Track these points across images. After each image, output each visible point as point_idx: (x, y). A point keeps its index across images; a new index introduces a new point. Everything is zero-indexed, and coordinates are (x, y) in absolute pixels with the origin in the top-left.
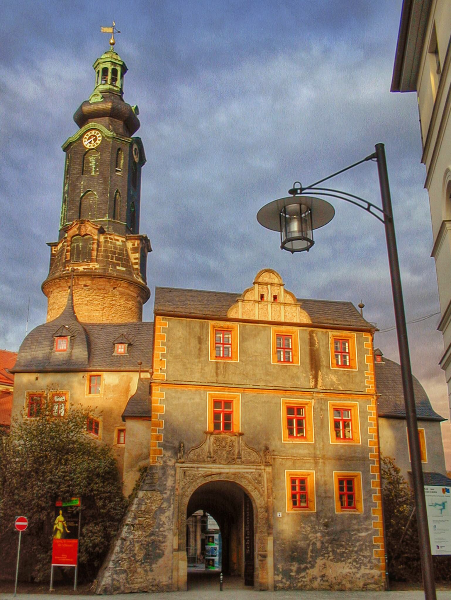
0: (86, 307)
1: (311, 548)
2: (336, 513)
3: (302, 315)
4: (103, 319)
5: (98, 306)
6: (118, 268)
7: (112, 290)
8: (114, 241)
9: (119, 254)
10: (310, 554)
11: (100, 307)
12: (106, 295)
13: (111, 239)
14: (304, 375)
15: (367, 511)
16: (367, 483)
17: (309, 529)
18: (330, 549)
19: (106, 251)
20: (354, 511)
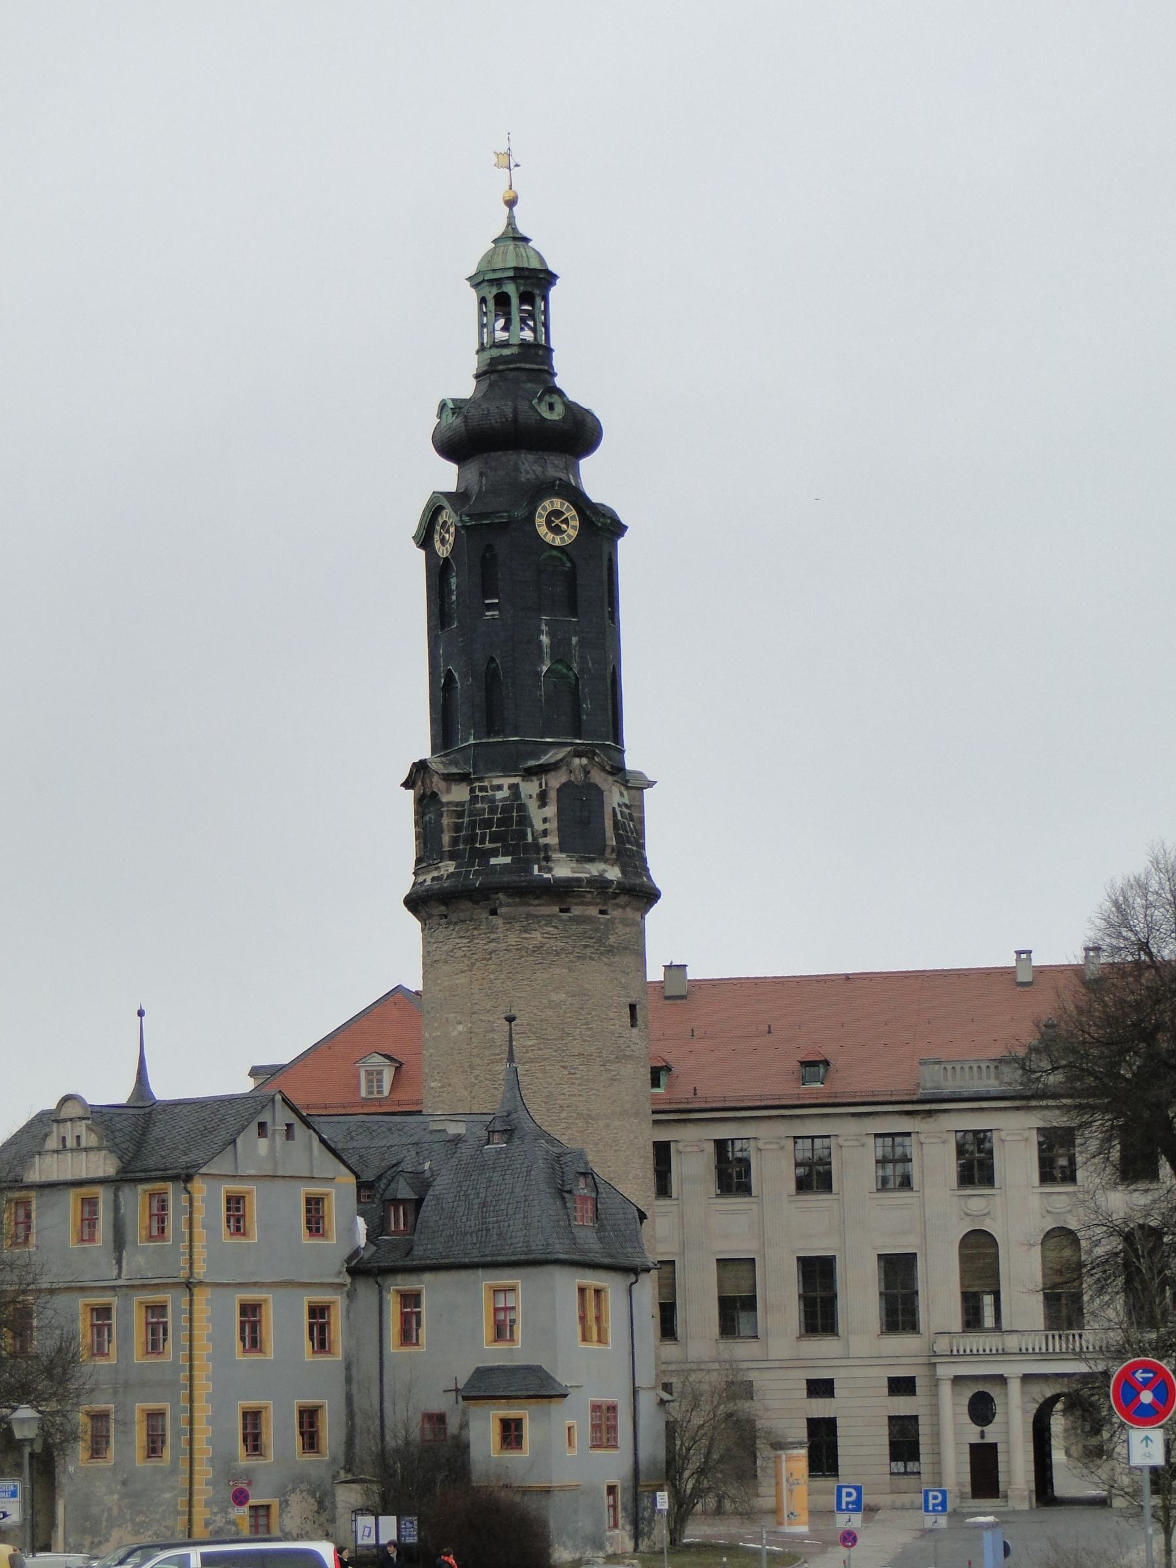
0: (446, 967)
1: (106, 1515)
2: (137, 1465)
3: (108, 1162)
4: (473, 991)
5: (463, 962)
6: (493, 861)
7: (487, 918)
8: (490, 793)
9: (501, 822)
10: (104, 1524)
11: (467, 962)
12: (476, 932)
13: (482, 789)
14: (106, 1260)
15: (175, 1461)
16: (175, 1419)
17: (104, 1489)
18: (128, 1517)
19: (472, 824)
20: (158, 1462)
